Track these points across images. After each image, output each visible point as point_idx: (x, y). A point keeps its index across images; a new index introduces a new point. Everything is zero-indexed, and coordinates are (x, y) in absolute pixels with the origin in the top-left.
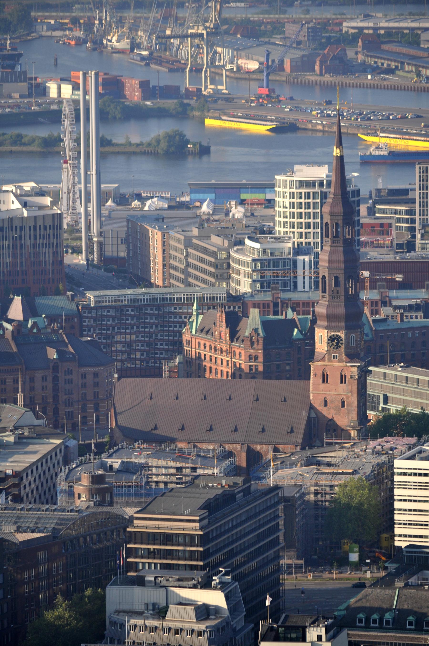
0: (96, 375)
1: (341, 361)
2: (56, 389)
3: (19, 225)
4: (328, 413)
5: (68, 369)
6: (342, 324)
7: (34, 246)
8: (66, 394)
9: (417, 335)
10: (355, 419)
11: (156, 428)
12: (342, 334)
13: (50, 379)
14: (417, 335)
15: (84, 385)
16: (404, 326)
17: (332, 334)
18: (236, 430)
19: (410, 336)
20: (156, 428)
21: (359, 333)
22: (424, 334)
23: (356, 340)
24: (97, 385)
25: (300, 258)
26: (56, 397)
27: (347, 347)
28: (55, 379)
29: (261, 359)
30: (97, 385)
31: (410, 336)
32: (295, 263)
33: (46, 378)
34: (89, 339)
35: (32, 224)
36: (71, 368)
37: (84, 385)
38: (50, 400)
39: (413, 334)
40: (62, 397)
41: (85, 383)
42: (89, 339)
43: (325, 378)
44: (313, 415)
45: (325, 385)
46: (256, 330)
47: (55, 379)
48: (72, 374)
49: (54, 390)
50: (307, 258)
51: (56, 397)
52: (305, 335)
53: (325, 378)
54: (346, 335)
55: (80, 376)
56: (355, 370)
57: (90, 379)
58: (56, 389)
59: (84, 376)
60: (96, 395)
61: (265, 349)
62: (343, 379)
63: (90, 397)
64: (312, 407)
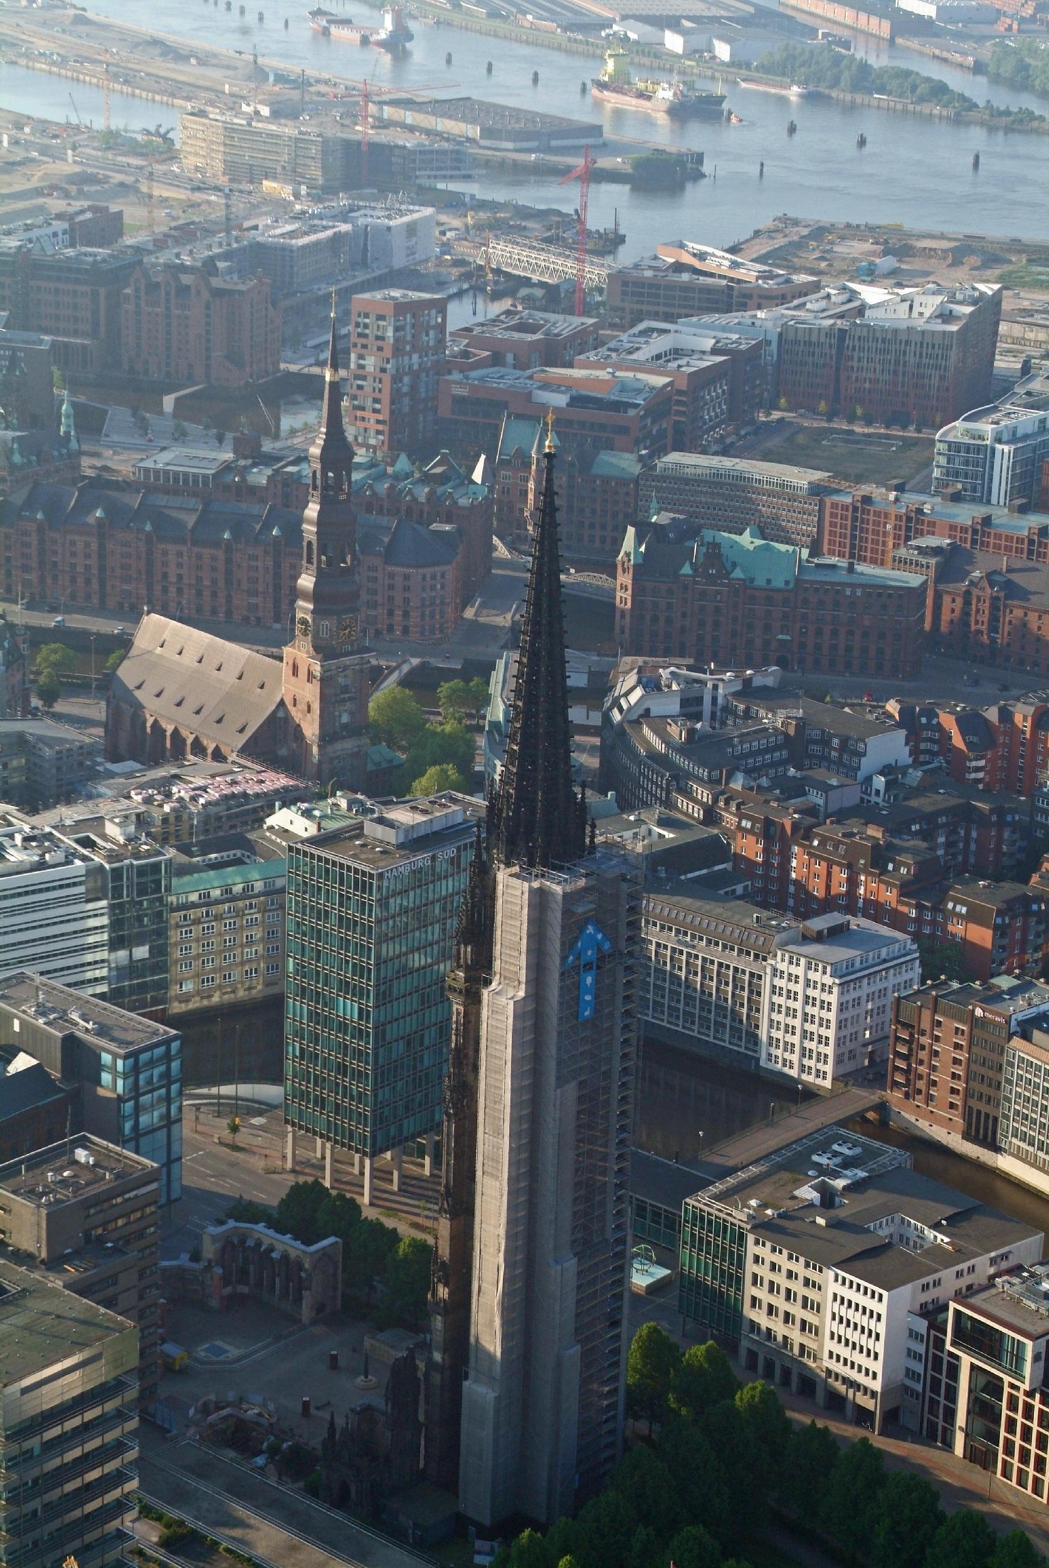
0: (407, 577)
1: (308, 652)
3: (904, 337)
4: (296, 714)
6: (311, 607)
7: (919, 366)
9: (859, 594)
10: (317, 732)
11: (139, 687)
12: (309, 618)
14: (859, 594)
15: (391, 587)
16: (853, 579)
18: (198, 712)
19: (848, 593)
20: (139, 687)
22: (869, 594)
24: (407, 589)
25: (999, 447)
27: (316, 637)
29: (630, 592)
30: (407, 589)
31: (848, 593)
32: (993, 450)
34: (448, 528)
35: (919, 339)
37: (391, 587)
39: (853, 592)
42: (447, 528)
43: (295, 671)
44: (281, 714)
45: (293, 679)
46: (628, 554)
50: (1006, 448)
52: (695, 570)
53: (295, 671)
54: (314, 620)
56: (318, 668)
57: (399, 581)
59: (392, 576)
60: (406, 601)
61: (634, 579)
62: (310, 676)
63: (398, 601)
64: (282, 703)
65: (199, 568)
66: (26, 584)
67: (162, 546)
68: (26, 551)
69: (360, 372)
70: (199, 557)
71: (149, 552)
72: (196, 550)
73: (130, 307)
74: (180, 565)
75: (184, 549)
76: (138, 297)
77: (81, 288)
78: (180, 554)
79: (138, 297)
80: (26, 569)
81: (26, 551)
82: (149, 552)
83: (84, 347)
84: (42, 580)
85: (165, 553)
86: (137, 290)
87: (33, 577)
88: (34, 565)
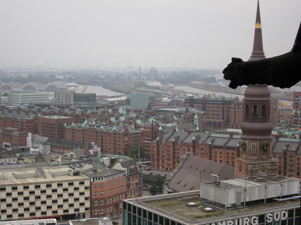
2: (285, 162)
5: (291, 155)
8: (289, 167)
13: (282, 158)
17: (243, 141)
21: (258, 143)
23: (256, 147)
26: (285, 167)
28: (285, 158)
33: (281, 157)
36: (292, 155)
38: (282, 168)
40: (288, 168)
41: (299, 163)
47: (285, 158)
48: (293, 157)
49: (284, 164)
51: (285, 167)
55: (297, 159)
58: (285, 162)
65: (228, 158)
66: (169, 164)
67: (214, 150)
68: (169, 153)
69: (296, 115)
70: (228, 154)
71: (210, 152)
72: (227, 151)
73: (233, 110)
74: (221, 157)
75: (222, 151)
76: (235, 107)
77: (219, 106)
78: (221, 153)
79: (235, 107)
80: (169, 159)
81: (169, 153)
82: (210, 152)
83: (220, 122)
84: (174, 163)
85: (216, 152)
86: (235, 105)
87: (171, 162)
88: (172, 158)
